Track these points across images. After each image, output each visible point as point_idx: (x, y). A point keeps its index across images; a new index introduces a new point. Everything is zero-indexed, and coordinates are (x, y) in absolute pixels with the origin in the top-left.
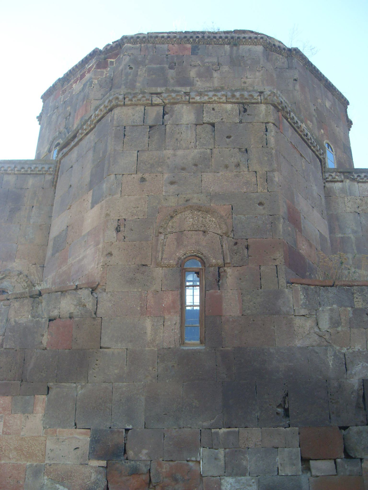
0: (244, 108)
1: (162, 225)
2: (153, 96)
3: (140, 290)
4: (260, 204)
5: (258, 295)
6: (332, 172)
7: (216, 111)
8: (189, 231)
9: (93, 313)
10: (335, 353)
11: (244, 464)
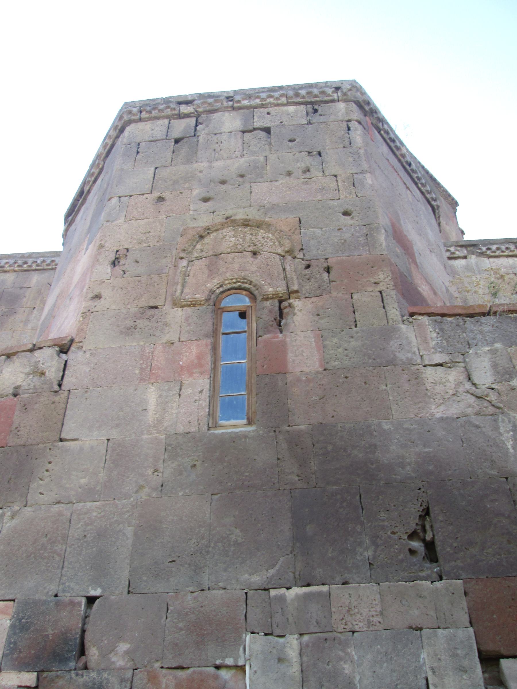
1: (186, 248)
3: (142, 343)
4: (346, 213)
6: (450, 246)
7: (272, 114)
8: (228, 253)
11: (346, 671)
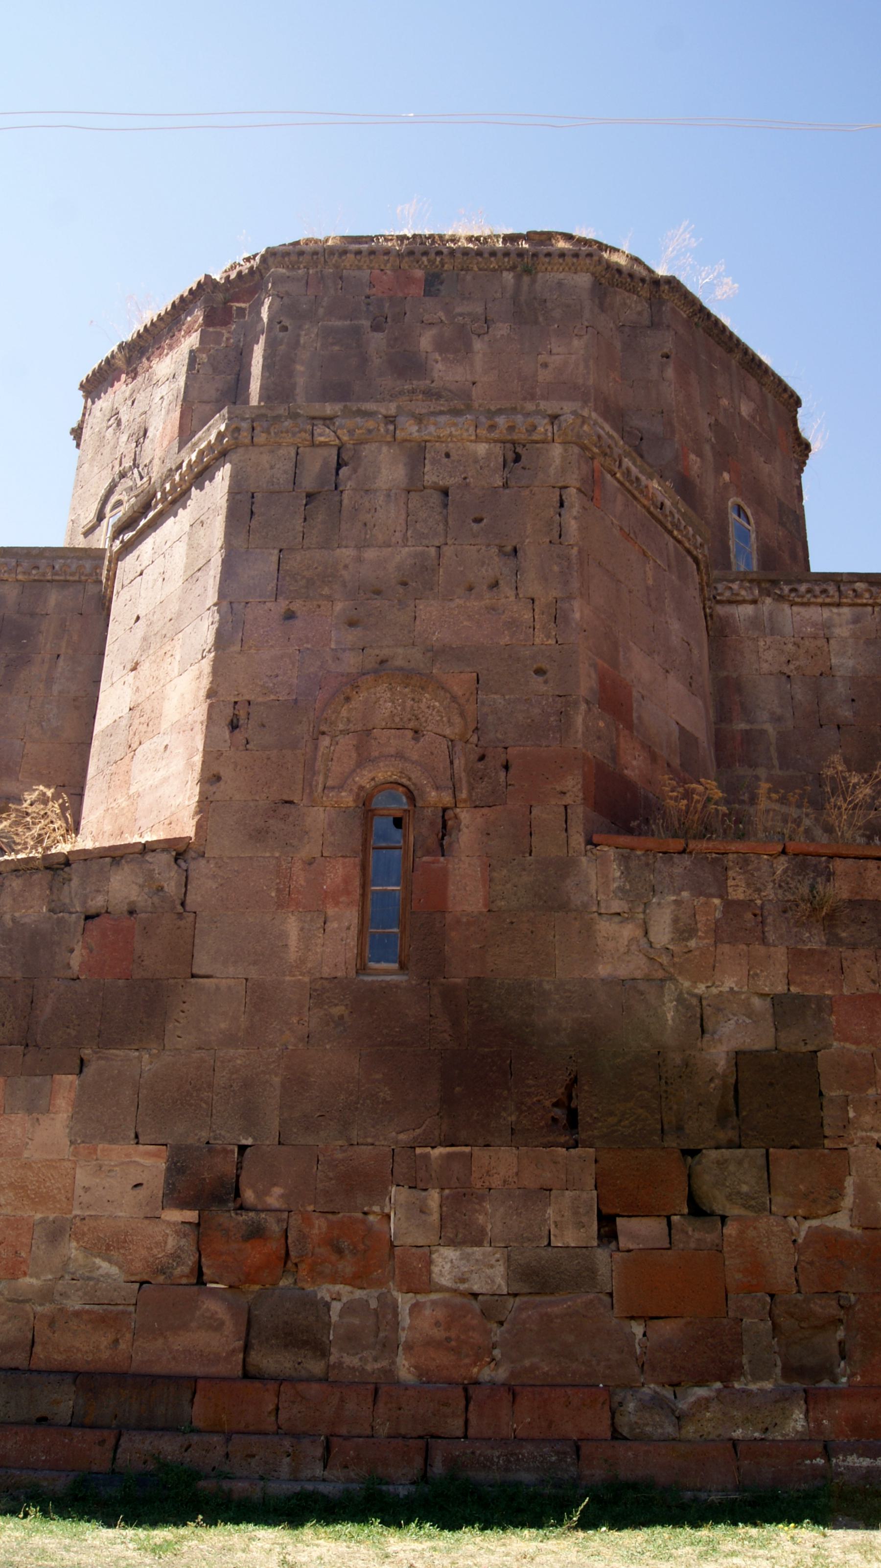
0: (514, 452)
2: (315, 422)
3: (277, 855)
4: (540, 672)
5: (524, 870)
7: (452, 458)
9: (178, 902)
10: (681, 993)
11: (480, 1221)
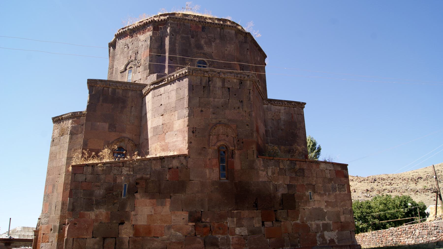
0: (241, 82)
2: (204, 72)
3: (203, 158)
4: (247, 125)
5: (247, 162)
9: (186, 166)
10: (273, 184)
